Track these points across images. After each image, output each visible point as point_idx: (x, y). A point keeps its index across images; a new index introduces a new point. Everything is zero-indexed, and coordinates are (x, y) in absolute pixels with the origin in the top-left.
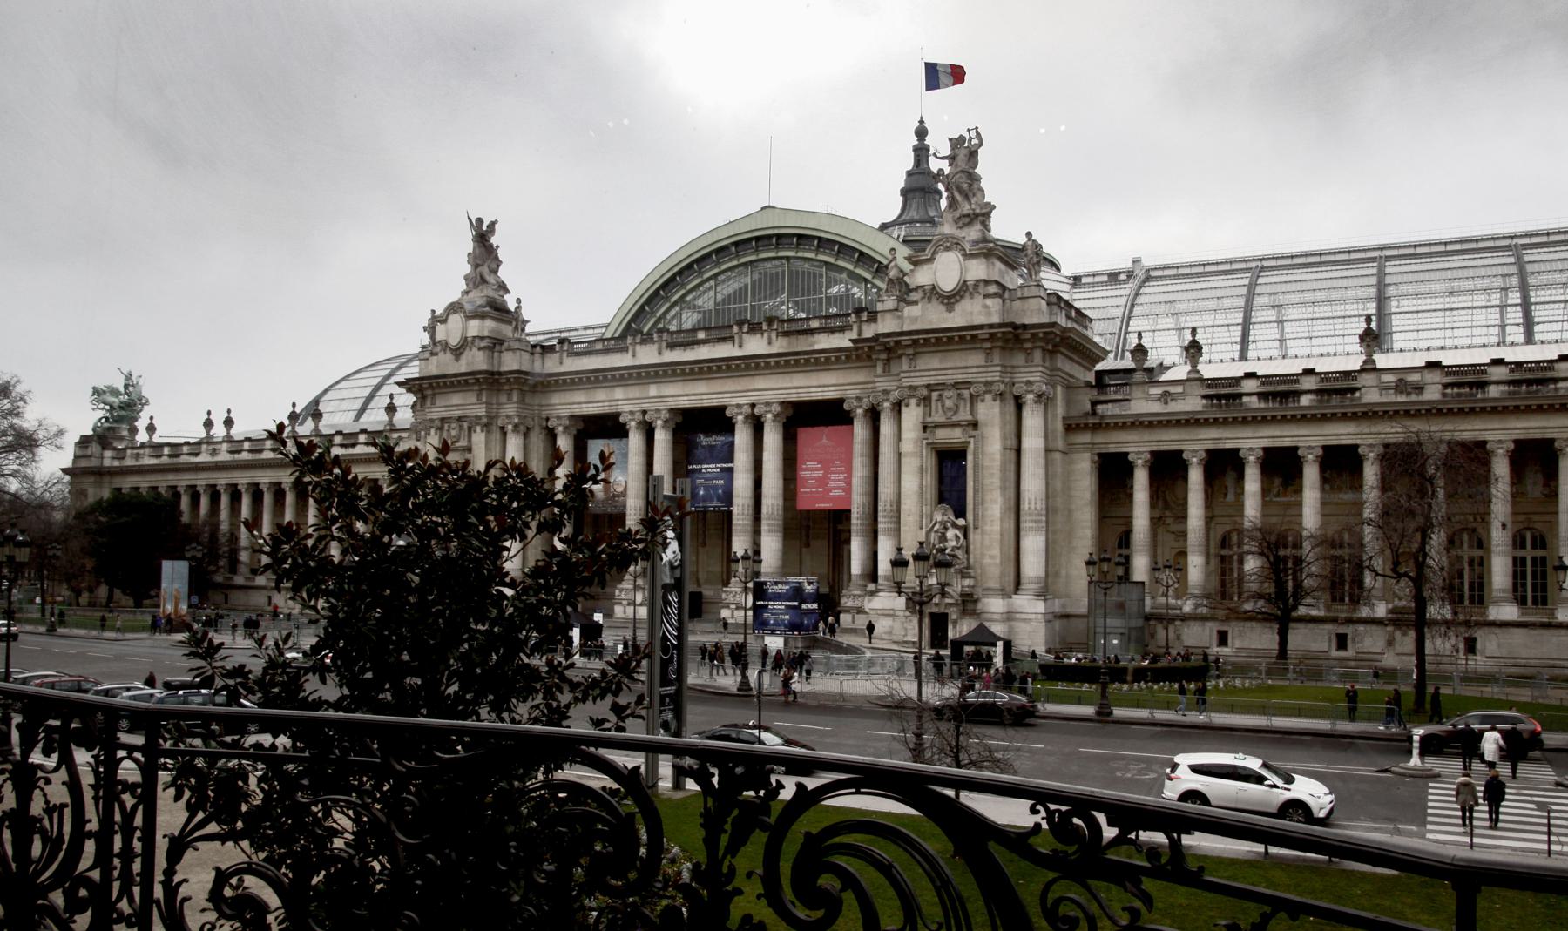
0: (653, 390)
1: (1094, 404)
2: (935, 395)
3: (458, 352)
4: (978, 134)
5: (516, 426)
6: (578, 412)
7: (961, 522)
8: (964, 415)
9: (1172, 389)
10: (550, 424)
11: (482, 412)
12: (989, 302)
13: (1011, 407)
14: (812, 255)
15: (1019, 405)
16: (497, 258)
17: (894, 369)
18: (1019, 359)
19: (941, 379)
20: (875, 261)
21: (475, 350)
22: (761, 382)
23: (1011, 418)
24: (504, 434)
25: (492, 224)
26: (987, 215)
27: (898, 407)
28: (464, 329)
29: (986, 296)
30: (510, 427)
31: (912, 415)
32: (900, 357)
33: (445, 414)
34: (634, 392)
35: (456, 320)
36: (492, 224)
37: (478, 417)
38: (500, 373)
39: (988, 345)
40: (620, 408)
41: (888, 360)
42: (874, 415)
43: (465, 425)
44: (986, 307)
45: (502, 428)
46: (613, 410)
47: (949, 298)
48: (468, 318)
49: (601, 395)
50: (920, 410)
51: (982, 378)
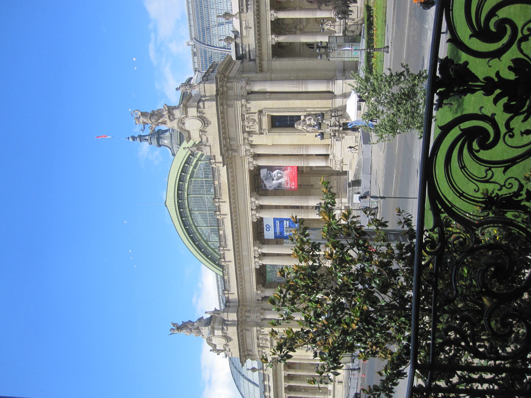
1: (250, 60)
2: (247, 129)
3: (228, 339)
5: (261, 314)
7: (302, 118)
8: (256, 117)
9: (244, 26)
11: (255, 329)
12: (206, 106)
13: (252, 96)
14: (187, 184)
15: (252, 93)
16: (187, 322)
17: (234, 148)
18: (231, 92)
20: (189, 157)
23: (257, 96)
25: (174, 324)
26: (168, 107)
27: (252, 146)
28: (219, 336)
29: (204, 108)
30: (261, 317)
31: (256, 139)
32: (231, 145)
33: (256, 345)
35: (215, 341)
36: (174, 324)
38: (238, 321)
39: (225, 107)
41: (232, 150)
42: (257, 156)
43: (260, 336)
44: (209, 107)
45: (262, 320)
47: (205, 124)
48: (214, 335)
51: (239, 109)
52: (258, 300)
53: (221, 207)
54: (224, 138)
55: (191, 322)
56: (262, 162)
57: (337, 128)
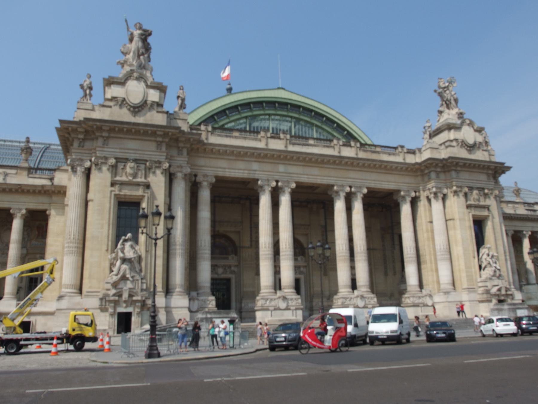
0: (281, 168)
6: (221, 173)
10: (199, 179)
11: (163, 159)
16: (149, 57)
19: (471, 185)
28: (146, 95)
33: (120, 155)
34: (268, 167)
40: (256, 176)
43: (142, 167)
44: (484, 155)
46: (251, 176)
49: (241, 165)
52: (196, 176)
53: (349, 149)
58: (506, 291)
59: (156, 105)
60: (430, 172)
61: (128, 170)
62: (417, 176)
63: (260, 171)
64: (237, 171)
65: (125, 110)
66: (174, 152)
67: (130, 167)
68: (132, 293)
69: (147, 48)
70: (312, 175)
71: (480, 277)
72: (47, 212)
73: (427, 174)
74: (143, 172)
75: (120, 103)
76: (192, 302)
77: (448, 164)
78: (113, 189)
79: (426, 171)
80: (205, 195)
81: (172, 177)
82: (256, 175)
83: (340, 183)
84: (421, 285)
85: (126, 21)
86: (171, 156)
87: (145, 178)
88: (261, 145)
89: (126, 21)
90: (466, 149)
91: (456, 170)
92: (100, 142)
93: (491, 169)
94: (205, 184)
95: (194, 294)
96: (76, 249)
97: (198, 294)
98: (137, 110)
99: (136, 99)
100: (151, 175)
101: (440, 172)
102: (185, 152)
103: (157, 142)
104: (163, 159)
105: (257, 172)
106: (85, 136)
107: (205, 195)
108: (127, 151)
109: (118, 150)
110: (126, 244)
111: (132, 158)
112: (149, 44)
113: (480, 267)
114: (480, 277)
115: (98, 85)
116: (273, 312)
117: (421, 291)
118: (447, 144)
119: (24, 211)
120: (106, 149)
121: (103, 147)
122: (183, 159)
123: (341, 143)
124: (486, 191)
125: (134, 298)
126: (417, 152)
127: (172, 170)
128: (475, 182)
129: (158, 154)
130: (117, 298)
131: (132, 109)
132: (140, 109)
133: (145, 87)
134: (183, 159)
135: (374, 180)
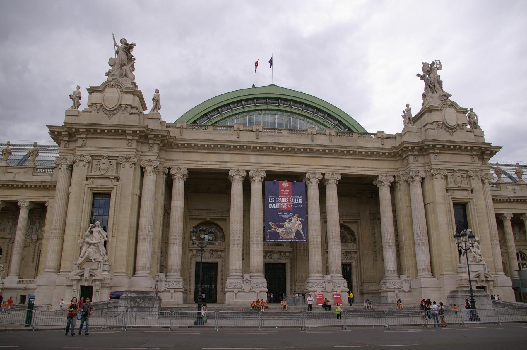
0: (253, 159)
3: (111, 112)
4: (440, 62)
6: (194, 166)
11: (132, 154)
16: (133, 66)
19: (452, 167)
21: (126, 114)
22: (326, 162)
24: (142, 174)
31: (438, 185)
34: (238, 158)
37: (127, 158)
40: (227, 167)
43: (114, 162)
46: (223, 167)
49: (213, 157)
50: (444, 181)
52: (169, 169)
53: (323, 137)
54: (443, 146)
55: (133, 71)
56: (385, 193)
57: (483, 278)
58: (486, 277)
59: (129, 107)
60: (408, 156)
61: (102, 166)
62: (397, 161)
63: (231, 162)
64: (209, 163)
65: (101, 113)
66: (145, 148)
67: (104, 163)
68: (91, 275)
69: (131, 59)
70: (284, 164)
71: (460, 263)
72: (46, 205)
73: (405, 157)
74: (115, 167)
75: (98, 108)
76: (159, 283)
77: (425, 147)
78: (87, 183)
79: (404, 156)
80: (179, 186)
81: (144, 171)
82: (227, 166)
83: (312, 171)
84: (400, 270)
85: (114, 38)
86: (142, 152)
87: (117, 172)
88: (234, 138)
89: (114, 38)
90: (448, 131)
91: (434, 153)
92: (79, 143)
93: (475, 150)
94: (179, 176)
95: (162, 276)
96: (59, 235)
97: (167, 276)
98: (112, 113)
99: (110, 105)
100: (122, 169)
101: (417, 155)
102: (156, 148)
103: (128, 139)
104: (132, 154)
105: (228, 164)
106: (69, 138)
107: (179, 186)
108: (101, 149)
109: (94, 149)
110: (93, 229)
111: (105, 155)
112: (132, 56)
113: (460, 252)
114: (460, 263)
115: (85, 95)
116: (238, 294)
117: (399, 277)
118: (429, 126)
119: (28, 204)
120: (83, 149)
121: (82, 147)
122: (153, 154)
123: (333, 133)
124: (470, 173)
125: (93, 278)
126: (398, 137)
127: (143, 164)
128: (456, 164)
129: (128, 150)
130: (79, 278)
131: (108, 113)
132: (115, 112)
133: (120, 92)
134: (153, 154)
135: (349, 167)
